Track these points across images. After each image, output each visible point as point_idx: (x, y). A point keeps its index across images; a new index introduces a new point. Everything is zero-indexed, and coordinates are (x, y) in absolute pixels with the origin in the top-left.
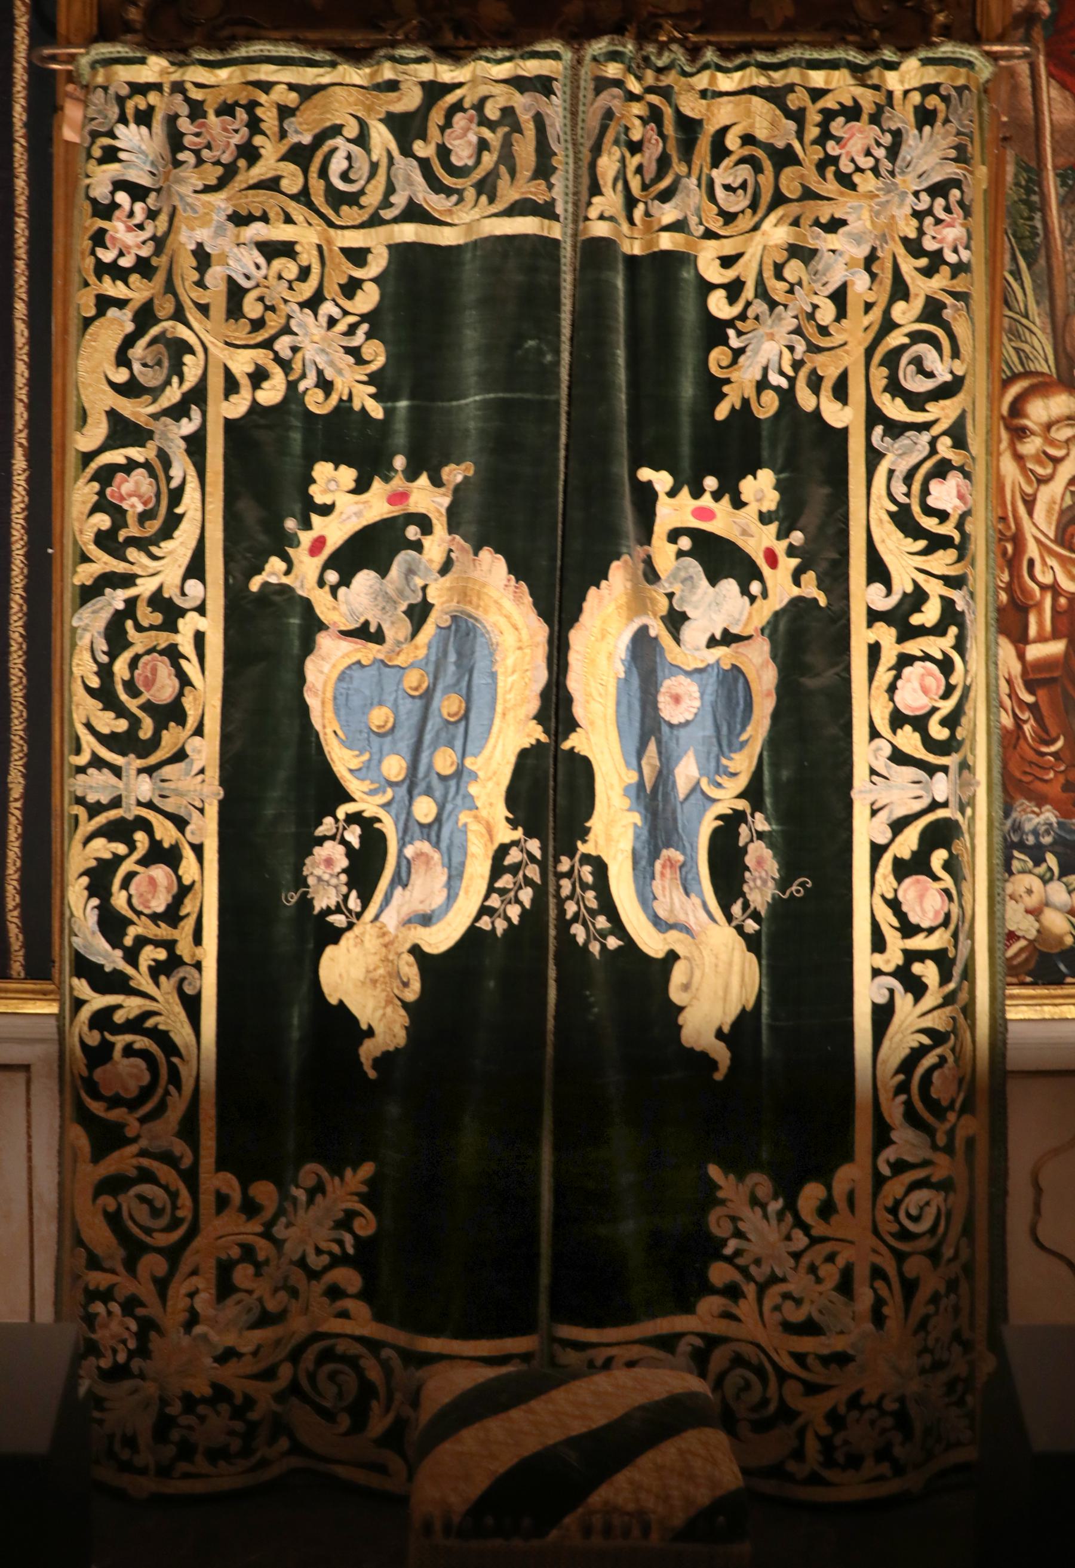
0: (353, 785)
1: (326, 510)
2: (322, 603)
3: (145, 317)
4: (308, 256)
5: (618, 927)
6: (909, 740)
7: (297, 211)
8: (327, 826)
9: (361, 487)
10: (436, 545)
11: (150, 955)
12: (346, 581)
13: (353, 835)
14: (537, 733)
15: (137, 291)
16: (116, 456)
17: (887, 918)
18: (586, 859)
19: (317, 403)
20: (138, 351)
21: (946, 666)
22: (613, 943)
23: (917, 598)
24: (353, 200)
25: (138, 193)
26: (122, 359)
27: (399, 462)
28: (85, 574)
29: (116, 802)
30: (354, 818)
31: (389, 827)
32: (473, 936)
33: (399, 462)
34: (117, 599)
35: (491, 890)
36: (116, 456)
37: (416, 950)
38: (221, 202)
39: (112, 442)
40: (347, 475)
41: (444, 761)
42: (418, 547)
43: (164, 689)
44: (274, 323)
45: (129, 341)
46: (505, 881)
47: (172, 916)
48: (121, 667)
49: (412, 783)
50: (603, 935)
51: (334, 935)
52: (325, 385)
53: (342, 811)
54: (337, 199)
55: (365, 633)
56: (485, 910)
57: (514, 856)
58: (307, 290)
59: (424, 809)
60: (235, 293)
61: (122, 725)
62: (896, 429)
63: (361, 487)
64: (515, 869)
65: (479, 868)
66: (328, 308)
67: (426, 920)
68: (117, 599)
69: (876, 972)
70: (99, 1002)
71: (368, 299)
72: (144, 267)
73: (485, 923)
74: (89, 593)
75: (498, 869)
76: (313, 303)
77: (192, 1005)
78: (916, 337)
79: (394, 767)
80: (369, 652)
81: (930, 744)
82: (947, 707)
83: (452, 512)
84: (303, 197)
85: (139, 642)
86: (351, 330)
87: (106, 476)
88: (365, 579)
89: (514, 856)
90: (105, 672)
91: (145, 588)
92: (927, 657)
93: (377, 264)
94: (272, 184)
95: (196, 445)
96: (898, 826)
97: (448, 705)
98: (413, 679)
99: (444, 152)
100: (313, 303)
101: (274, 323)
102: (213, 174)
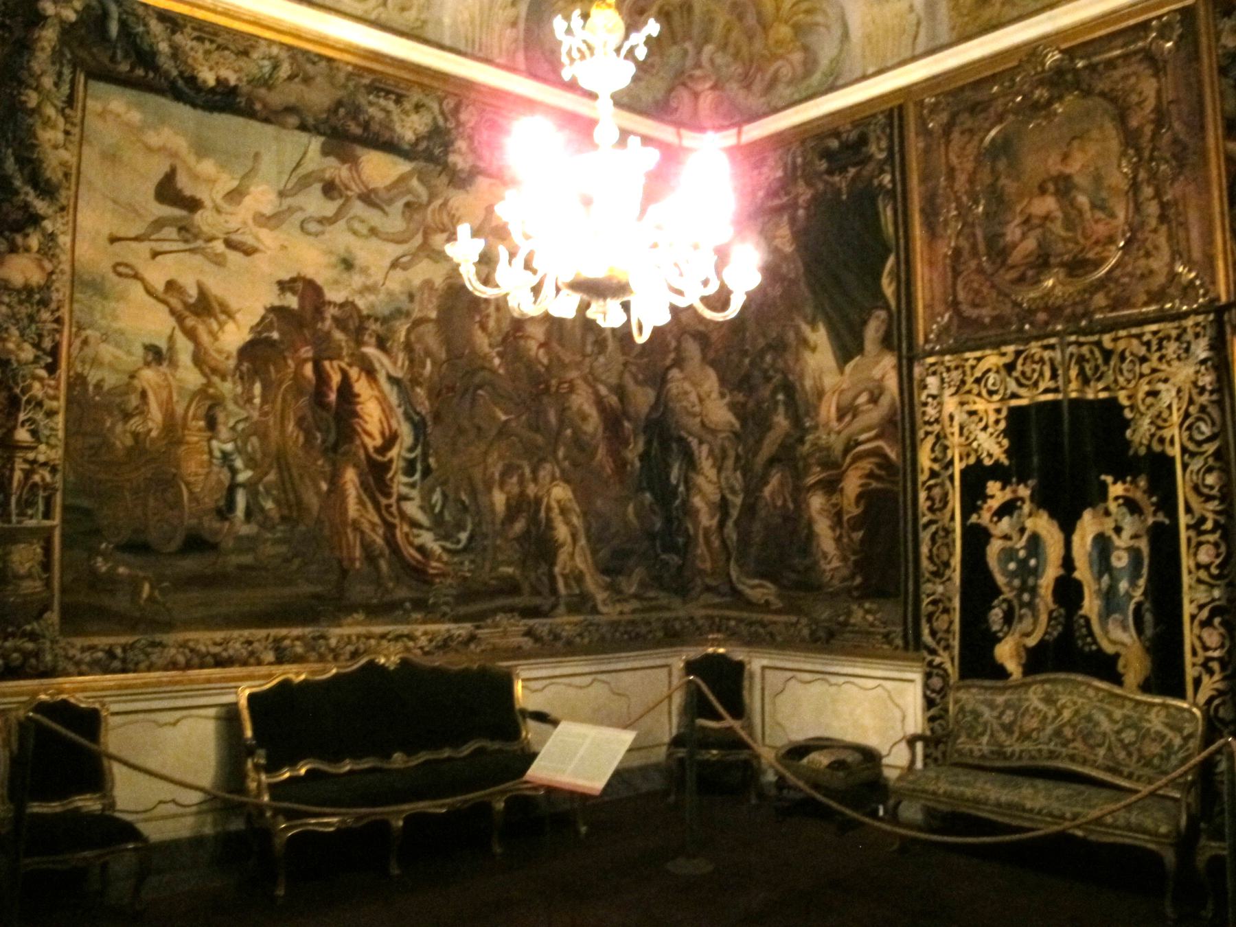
0: (1005, 589)
1: (992, 497)
2: (992, 528)
3: (938, 437)
4: (981, 414)
5: (1095, 642)
6: (1203, 574)
7: (977, 399)
8: (996, 602)
9: (1003, 488)
10: (1026, 508)
11: (943, 643)
12: (1000, 520)
13: (1005, 606)
14: (1061, 572)
15: (936, 428)
16: (932, 482)
17: (1198, 644)
18: (1082, 617)
19: (988, 462)
20: (937, 448)
21: (1216, 545)
22: (1094, 647)
23: (1203, 520)
24: (996, 392)
25: (934, 397)
26: (933, 450)
27: (1014, 480)
28: (924, 520)
29: (933, 594)
30: (1005, 600)
31: (1015, 603)
32: (1042, 643)
33: (1014, 480)
34: (933, 528)
35: (1048, 625)
36: (932, 482)
37: (1024, 646)
38: (956, 399)
39: (930, 479)
40: (998, 485)
41: (1031, 581)
42: (1021, 508)
43: (945, 557)
44: (972, 437)
45: (935, 444)
46: (1053, 623)
47: (948, 631)
48: (935, 550)
49: (1023, 588)
50: (1090, 644)
51: (999, 640)
52: (990, 455)
53: (1001, 598)
54: (991, 393)
55: (1006, 537)
56: (1046, 633)
57: (1055, 614)
58: (982, 425)
59: (1026, 597)
60: (962, 428)
61: (935, 569)
62: (1193, 455)
63: (1003, 488)
64: (1056, 618)
65: (1044, 618)
66: (990, 430)
67: (1028, 635)
68: (933, 528)
69: (1194, 665)
70: (929, 658)
71: (1002, 425)
72: (937, 421)
73: (1047, 637)
74: (926, 526)
75: (1050, 618)
76: (985, 428)
77: (952, 660)
78: (1199, 419)
79: (1017, 582)
80: (1009, 544)
81: (1212, 576)
82: (1218, 561)
83: (1032, 497)
84: (979, 395)
85: (939, 542)
86: (998, 436)
87: (929, 488)
88: (1006, 520)
89: (1055, 614)
90: (931, 551)
91: (940, 524)
92: (1208, 542)
93: (1004, 413)
94: (969, 392)
95: (951, 478)
96: (1201, 607)
97: (1033, 562)
98: (1022, 554)
99: (1023, 373)
100: (985, 428)
101: (972, 437)
102: (953, 390)
